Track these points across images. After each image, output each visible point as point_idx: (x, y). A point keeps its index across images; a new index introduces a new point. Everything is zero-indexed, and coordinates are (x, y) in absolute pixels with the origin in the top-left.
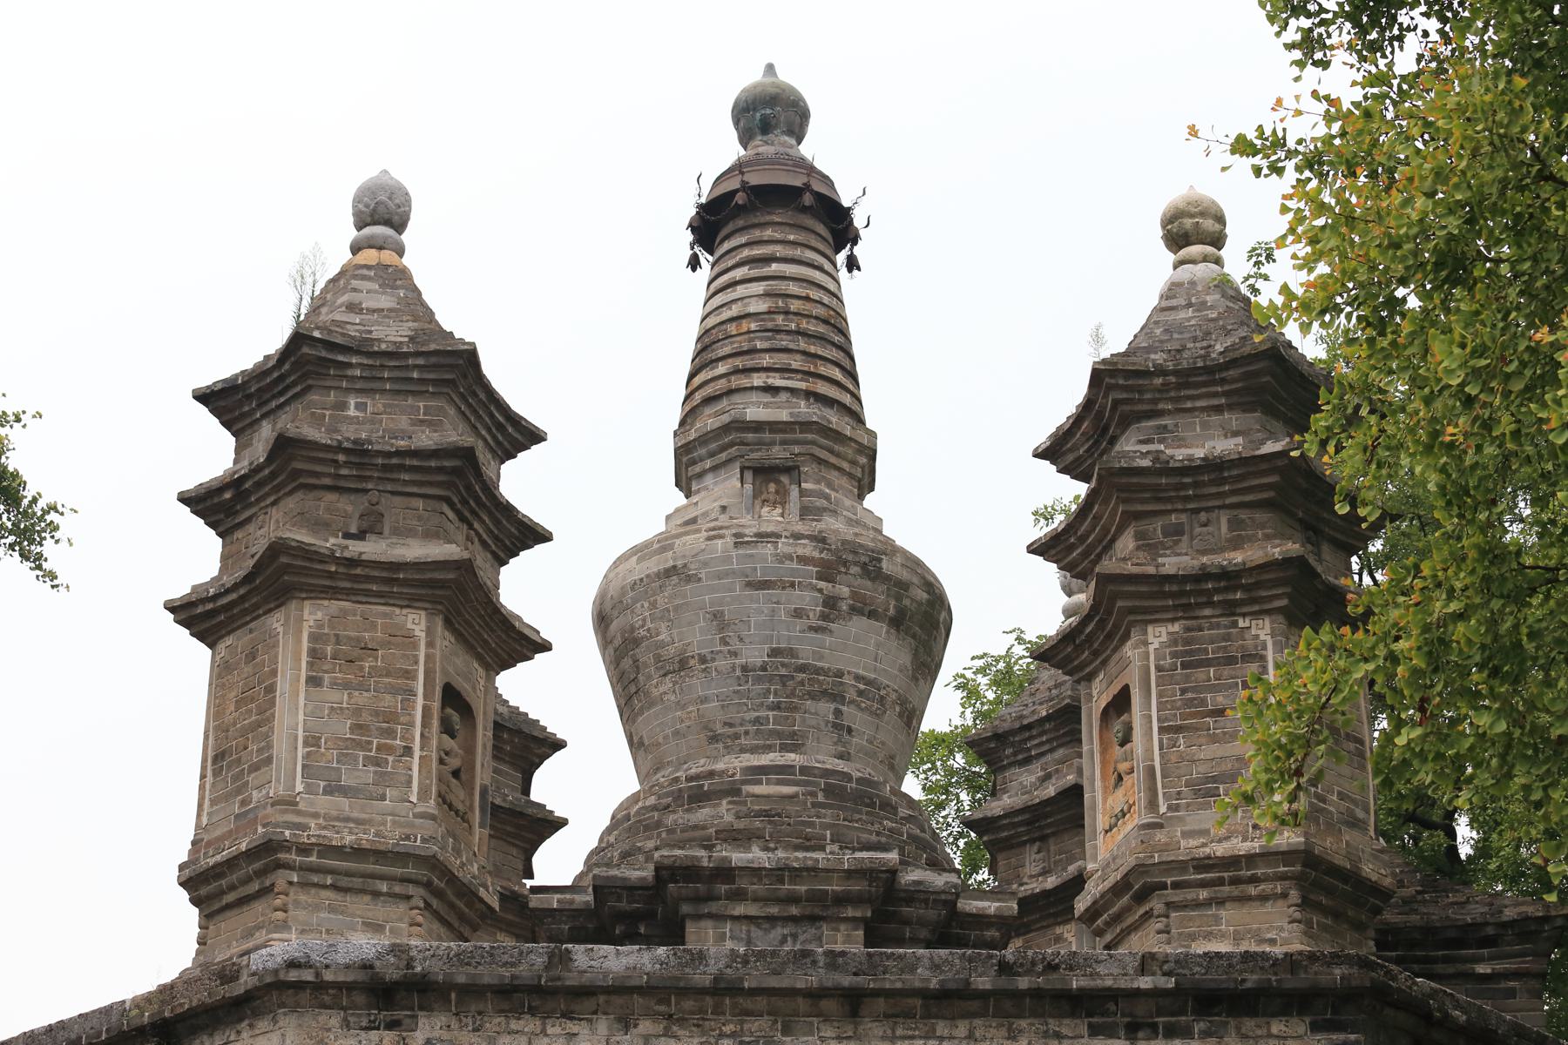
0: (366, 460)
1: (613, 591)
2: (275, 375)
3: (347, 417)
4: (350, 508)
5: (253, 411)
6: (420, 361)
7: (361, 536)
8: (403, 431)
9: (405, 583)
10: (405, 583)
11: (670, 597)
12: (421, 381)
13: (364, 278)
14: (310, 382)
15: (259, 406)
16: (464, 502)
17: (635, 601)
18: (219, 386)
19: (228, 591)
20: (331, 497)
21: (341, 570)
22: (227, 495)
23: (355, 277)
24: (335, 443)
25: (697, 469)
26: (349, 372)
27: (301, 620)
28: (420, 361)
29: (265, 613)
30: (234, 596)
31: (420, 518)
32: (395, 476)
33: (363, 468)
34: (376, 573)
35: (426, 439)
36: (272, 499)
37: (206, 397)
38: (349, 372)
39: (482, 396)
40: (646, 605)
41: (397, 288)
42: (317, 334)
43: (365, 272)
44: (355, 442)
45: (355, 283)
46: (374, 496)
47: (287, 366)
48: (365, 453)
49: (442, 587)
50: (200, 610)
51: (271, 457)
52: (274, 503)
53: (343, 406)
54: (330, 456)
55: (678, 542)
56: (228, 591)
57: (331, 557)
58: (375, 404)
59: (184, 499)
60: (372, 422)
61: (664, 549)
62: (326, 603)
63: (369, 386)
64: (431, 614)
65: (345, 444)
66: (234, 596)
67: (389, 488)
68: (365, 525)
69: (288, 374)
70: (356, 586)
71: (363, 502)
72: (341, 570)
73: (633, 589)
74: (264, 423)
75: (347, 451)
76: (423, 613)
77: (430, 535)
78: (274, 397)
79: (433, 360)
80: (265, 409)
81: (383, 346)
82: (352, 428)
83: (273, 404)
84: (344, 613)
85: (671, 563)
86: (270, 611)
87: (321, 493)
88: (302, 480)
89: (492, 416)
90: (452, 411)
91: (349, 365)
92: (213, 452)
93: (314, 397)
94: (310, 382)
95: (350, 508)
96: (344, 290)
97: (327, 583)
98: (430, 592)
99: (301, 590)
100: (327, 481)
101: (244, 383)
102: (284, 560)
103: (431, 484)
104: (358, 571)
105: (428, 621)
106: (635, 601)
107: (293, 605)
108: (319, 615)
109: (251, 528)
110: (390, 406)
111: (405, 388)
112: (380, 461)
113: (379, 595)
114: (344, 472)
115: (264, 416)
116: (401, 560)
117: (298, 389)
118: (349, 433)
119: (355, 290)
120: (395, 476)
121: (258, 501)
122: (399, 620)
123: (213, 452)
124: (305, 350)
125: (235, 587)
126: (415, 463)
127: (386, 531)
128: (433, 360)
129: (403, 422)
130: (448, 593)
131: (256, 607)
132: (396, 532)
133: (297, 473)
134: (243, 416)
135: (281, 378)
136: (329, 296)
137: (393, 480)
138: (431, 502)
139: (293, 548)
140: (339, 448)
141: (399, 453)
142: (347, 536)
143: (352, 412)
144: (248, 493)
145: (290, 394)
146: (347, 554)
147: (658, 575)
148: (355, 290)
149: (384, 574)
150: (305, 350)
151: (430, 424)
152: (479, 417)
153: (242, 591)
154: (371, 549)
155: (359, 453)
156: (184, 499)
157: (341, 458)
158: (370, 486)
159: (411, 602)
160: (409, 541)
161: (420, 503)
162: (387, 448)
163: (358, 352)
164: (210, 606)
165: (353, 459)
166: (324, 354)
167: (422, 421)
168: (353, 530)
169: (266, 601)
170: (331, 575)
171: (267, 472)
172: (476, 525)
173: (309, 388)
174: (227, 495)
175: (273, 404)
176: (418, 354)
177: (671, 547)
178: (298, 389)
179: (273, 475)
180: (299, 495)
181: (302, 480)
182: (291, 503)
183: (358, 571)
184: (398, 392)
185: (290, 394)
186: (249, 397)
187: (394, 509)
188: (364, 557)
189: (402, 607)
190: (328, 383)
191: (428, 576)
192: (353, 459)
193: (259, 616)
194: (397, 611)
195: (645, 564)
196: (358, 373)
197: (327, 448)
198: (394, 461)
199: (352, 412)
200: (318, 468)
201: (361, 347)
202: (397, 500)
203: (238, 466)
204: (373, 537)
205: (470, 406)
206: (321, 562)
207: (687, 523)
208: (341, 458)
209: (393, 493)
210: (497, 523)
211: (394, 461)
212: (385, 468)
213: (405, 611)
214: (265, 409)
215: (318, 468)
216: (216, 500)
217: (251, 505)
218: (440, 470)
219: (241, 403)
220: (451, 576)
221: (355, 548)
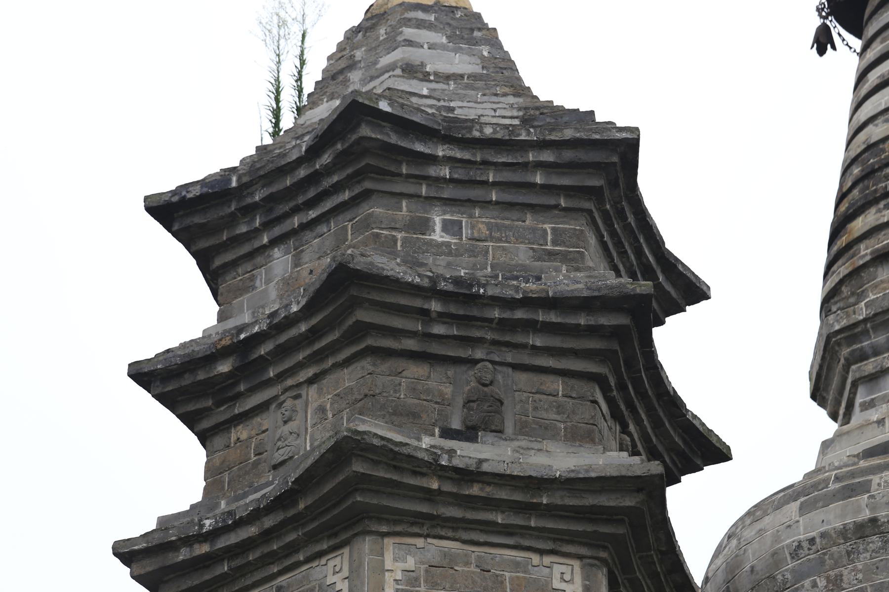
0: (475, 312)
1: (755, 556)
2: (302, 173)
3: (431, 243)
4: (448, 390)
5: (255, 233)
6: (548, 156)
7: (469, 434)
8: (524, 268)
9: (550, 511)
10: (550, 511)
11: (867, 571)
12: (546, 188)
13: (421, 24)
14: (368, 185)
15: (267, 225)
16: (622, 387)
17: (799, 576)
18: (196, 192)
19: (240, 523)
20: (416, 370)
21: (448, 487)
22: (224, 367)
23: (407, 22)
24: (426, 283)
25: (869, 366)
26: (432, 171)
27: (382, 570)
28: (548, 156)
29: (308, 560)
30: (252, 531)
31: (560, 409)
32: (519, 339)
33: (469, 321)
34: (503, 494)
35: (563, 281)
36: (310, 372)
37: (167, 210)
38: (432, 171)
39: (631, 219)
40: (822, 583)
41: (476, 42)
42: (384, 106)
43: (420, 15)
44: (457, 281)
45: (409, 32)
46: (485, 370)
47: (326, 158)
48: (474, 299)
49: (608, 521)
50: (183, 555)
51: (308, 310)
52: (311, 381)
53: (425, 226)
54: (418, 303)
55: (876, 479)
56: (240, 523)
57: (434, 467)
58: (475, 223)
59: (143, 374)
60: (472, 252)
61: (850, 492)
62: (420, 542)
63: (463, 194)
64: (589, 564)
65: (442, 285)
66: (252, 531)
67: (509, 358)
68: (475, 419)
69: (328, 171)
70: (470, 515)
71: (468, 378)
72: (448, 487)
73: (795, 555)
74: (277, 252)
75: (444, 296)
76: (577, 564)
77: (581, 436)
78: (296, 210)
79: (568, 155)
80: (277, 231)
81: (488, 131)
82: (443, 260)
83: (296, 221)
84: (449, 561)
85: (866, 514)
86: (320, 555)
87: (401, 364)
88: (370, 341)
89: (639, 253)
90: (592, 240)
91: (432, 159)
92: (180, 306)
93: (376, 209)
94: (368, 185)
95: (448, 390)
96: (392, 44)
97: (424, 508)
98: (590, 528)
99: (380, 520)
100: (410, 344)
101: (242, 187)
102: (358, 467)
103: (576, 354)
104: (475, 490)
105: (586, 577)
106: (799, 576)
107: (366, 545)
108: (410, 563)
109: (265, 421)
110: (499, 228)
111: (522, 199)
112: (496, 314)
113: (507, 530)
114: (438, 329)
115: (274, 243)
116: (545, 473)
117: (346, 195)
118: (443, 268)
119: (410, 43)
120: (519, 339)
121: (281, 377)
122: (535, 574)
123: (176, 302)
124: (365, 131)
125: (255, 515)
126: (553, 317)
127: (509, 429)
128: (568, 155)
129: (522, 254)
130: (621, 530)
131: (292, 548)
132: (524, 429)
133: (362, 330)
134: (237, 240)
135: (314, 178)
136: (359, 54)
137: (508, 344)
138: (572, 382)
139: (372, 448)
140: (432, 292)
141: (528, 302)
142: (448, 433)
143: (438, 235)
144: (264, 362)
145: (328, 205)
146: (456, 462)
147: (843, 533)
148: (410, 43)
149: (518, 497)
150: (365, 131)
151: (565, 258)
152: (623, 254)
153: (269, 522)
154: (490, 453)
155: (463, 297)
156: (143, 374)
157: (435, 306)
158: (479, 354)
159: (556, 544)
160: (548, 445)
161: (558, 385)
162: (509, 293)
163: (447, 139)
164: (204, 549)
165: (453, 309)
166: (394, 139)
167: (551, 254)
168: (456, 424)
169: (312, 538)
170: (429, 495)
171: (303, 328)
172: (632, 428)
173: (366, 195)
174: (224, 367)
175: (296, 221)
176: (543, 145)
177: (865, 488)
178: (346, 195)
179: (314, 334)
180: (366, 364)
181: (370, 341)
182: (348, 379)
183: (475, 490)
184: (511, 205)
185: (328, 205)
186: (249, 210)
187: (518, 390)
188: (486, 467)
189: (541, 552)
190: (398, 188)
191: (590, 500)
192: (453, 309)
193: (297, 565)
194: (535, 559)
195: (817, 516)
196: (446, 172)
197: (414, 290)
198: (520, 314)
199: (438, 235)
200: (397, 322)
201: (451, 132)
202: (522, 378)
203: (231, 324)
204: (490, 437)
205: (613, 234)
206: (415, 473)
207: (869, 453)
208: (435, 306)
209: (516, 367)
210: (657, 424)
211: (520, 314)
212: (504, 325)
213: (547, 560)
214: (277, 231)
215: (397, 322)
216: (201, 376)
217: (269, 383)
218: (593, 331)
219: (232, 220)
220: (629, 502)
221: (467, 453)
